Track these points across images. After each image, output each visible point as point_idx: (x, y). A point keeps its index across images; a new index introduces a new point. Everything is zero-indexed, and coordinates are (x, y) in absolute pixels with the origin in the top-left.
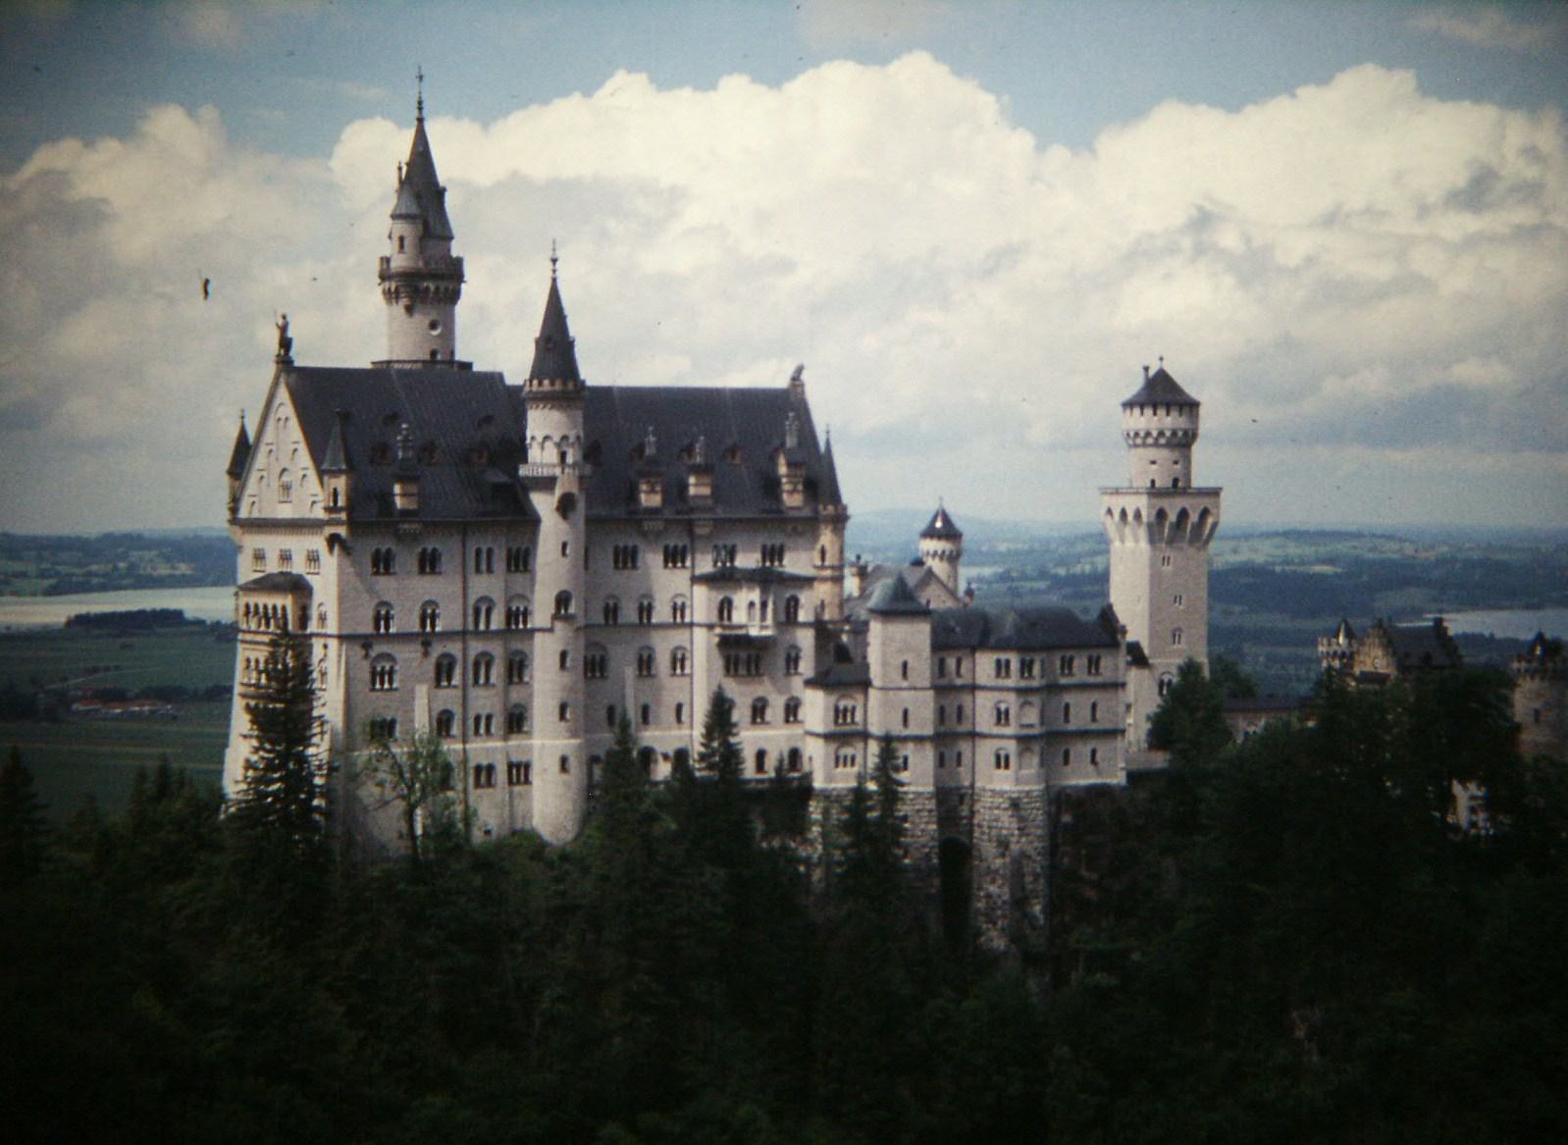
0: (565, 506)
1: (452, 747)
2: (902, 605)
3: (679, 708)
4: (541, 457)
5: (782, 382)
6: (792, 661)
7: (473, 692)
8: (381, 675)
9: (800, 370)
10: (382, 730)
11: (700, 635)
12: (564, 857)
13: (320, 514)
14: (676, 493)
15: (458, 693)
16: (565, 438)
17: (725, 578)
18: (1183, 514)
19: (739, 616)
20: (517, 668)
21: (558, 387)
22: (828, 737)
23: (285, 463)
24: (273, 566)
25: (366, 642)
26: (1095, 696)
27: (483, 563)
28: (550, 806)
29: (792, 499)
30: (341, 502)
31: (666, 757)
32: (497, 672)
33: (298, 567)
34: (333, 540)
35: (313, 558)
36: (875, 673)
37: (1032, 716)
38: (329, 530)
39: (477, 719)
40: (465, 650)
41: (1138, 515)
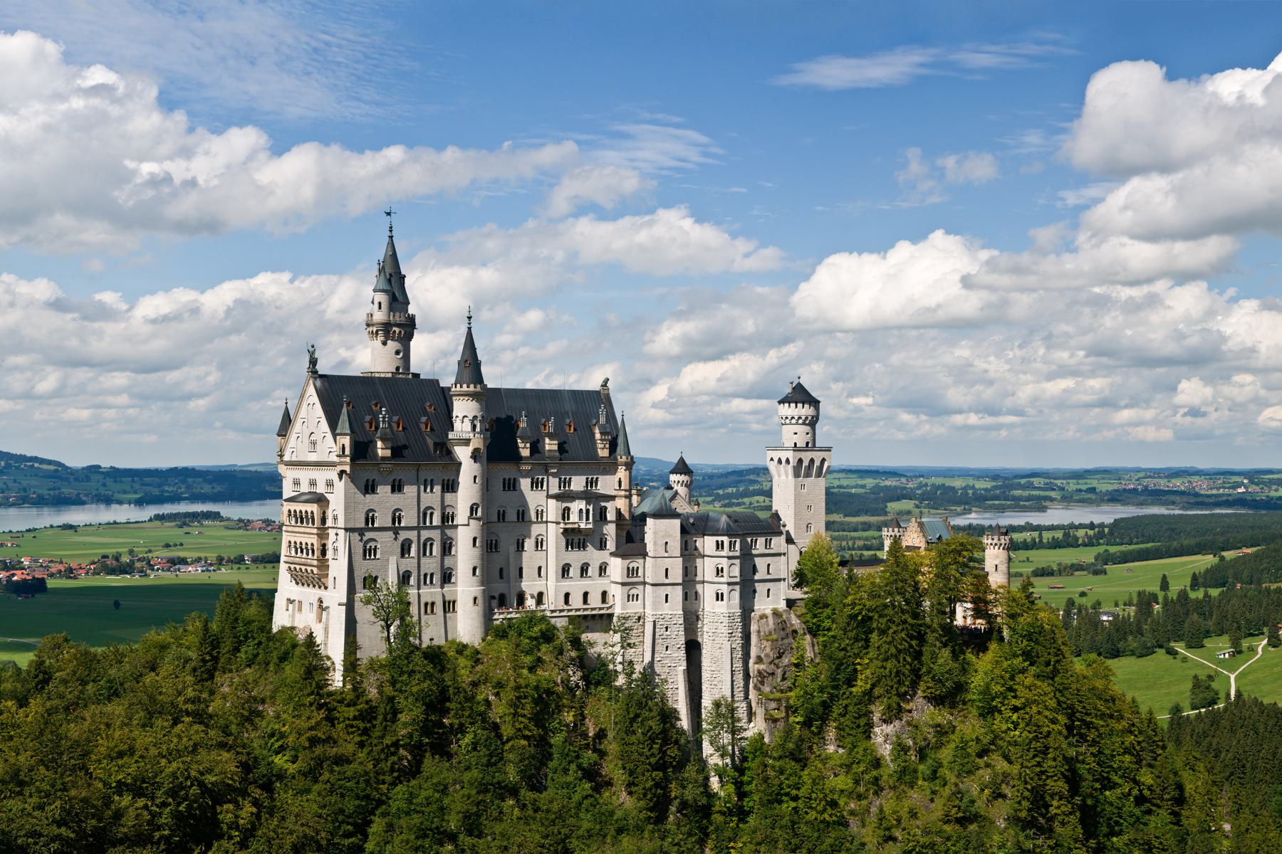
0: (475, 456)
3: (540, 568)
4: (461, 427)
5: (598, 388)
6: (602, 545)
7: (423, 560)
8: (369, 552)
10: (370, 582)
11: (552, 527)
13: (336, 459)
14: (536, 448)
15: (416, 561)
16: (475, 417)
17: (565, 496)
18: (812, 461)
19: (574, 517)
20: (447, 548)
21: (472, 388)
22: (623, 584)
25: (361, 532)
26: (769, 560)
28: (466, 626)
30: (347, 452)
31: (532, 597)
32: (436, 550)
34: (342, 473)
35: (330, 484)
36: (650, 548)
37: (736, 571)
38: (339, 468)
39: (425, 575)
40: (419, 536)
41: (788, 461)
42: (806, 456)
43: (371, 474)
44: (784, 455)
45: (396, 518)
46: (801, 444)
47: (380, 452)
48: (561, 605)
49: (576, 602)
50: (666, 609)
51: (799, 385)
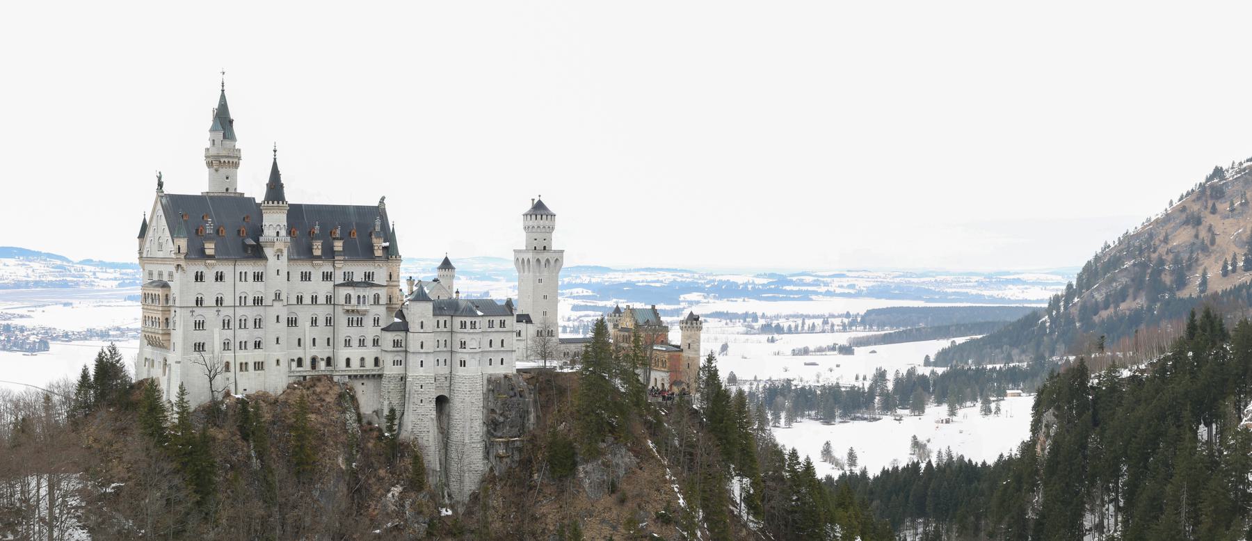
1: (228, 356)
2: (421, 297)
4: (269, 233)
9: (383, 199)
10: (199, 347)
12: (276, 401)
19: (354, 301)
20: (258, 323)
23: (160, 234)
24: (156, 278)
26: (502, 336)
27: (243, 277)
29: (378, 253)
32: (250, 324)
33: (165, 278)
35: (171, 275)
42: (543, 257)
43: (199, 267)
44: (526, 256)
45: (219, 301)
46: (540, 247)
47: (208, 252)
48: (342, 365)
49: (355, 364)
50: (421, 372)
51: (540, 202)
